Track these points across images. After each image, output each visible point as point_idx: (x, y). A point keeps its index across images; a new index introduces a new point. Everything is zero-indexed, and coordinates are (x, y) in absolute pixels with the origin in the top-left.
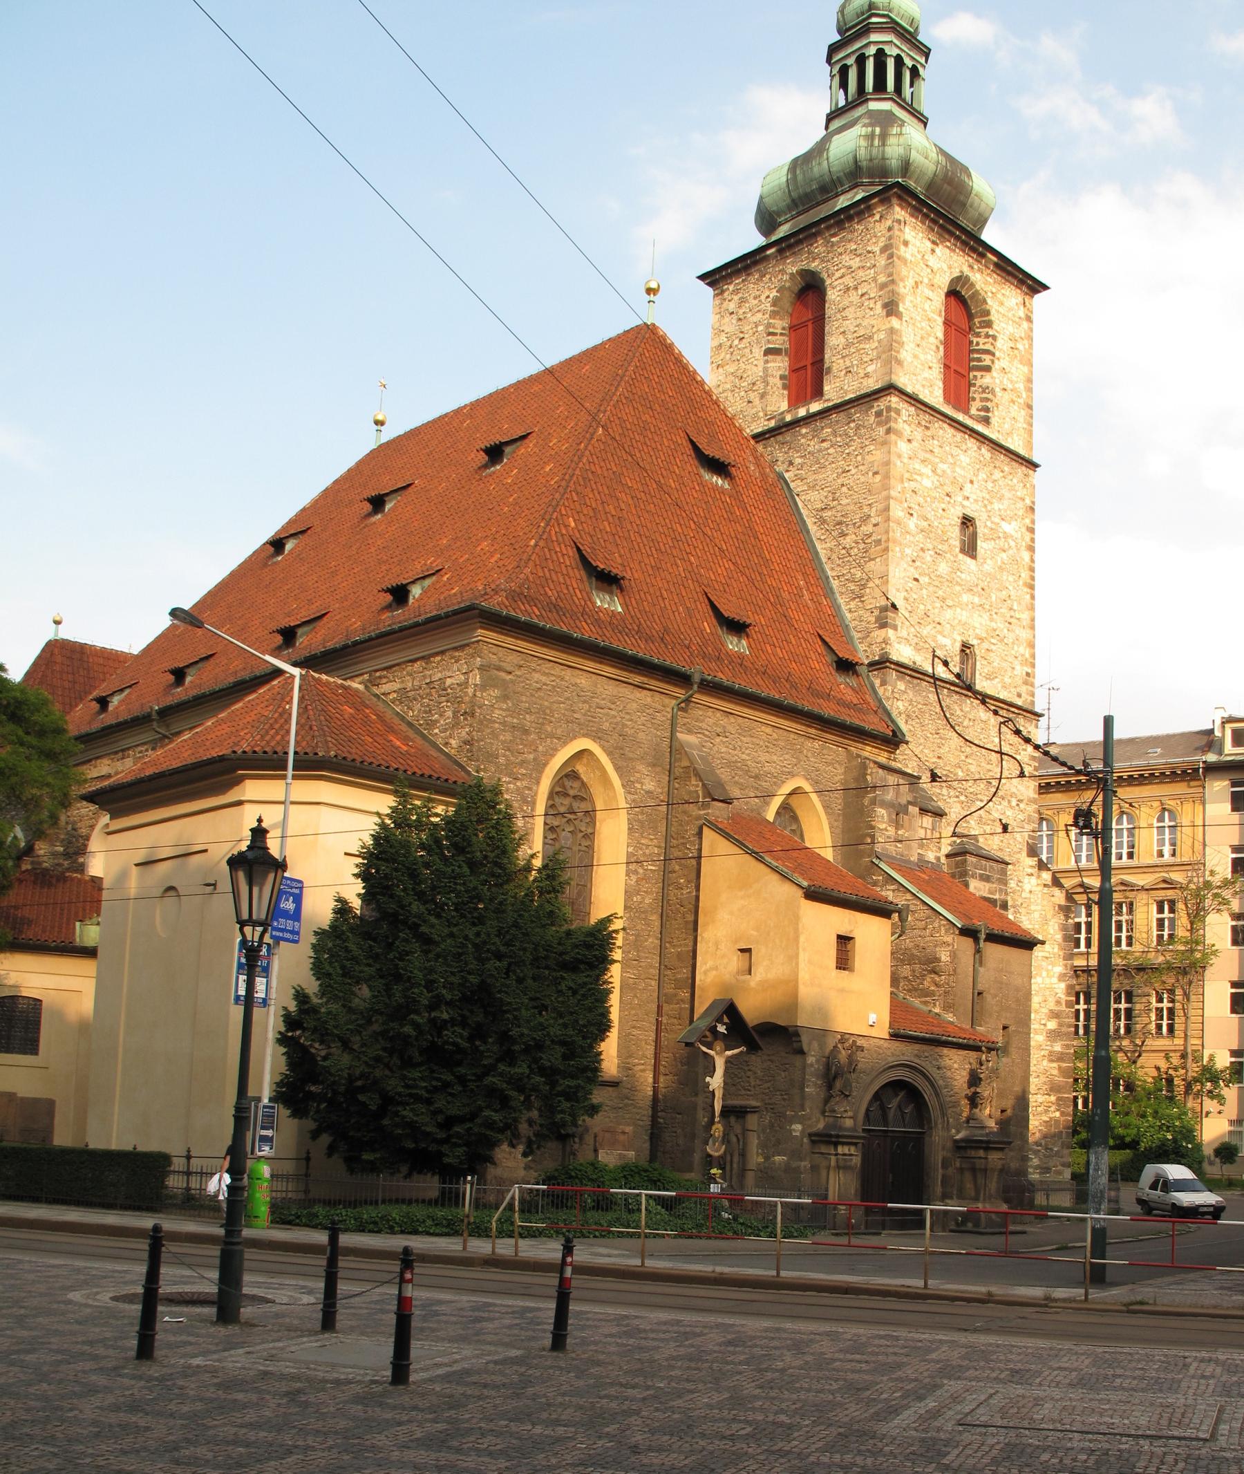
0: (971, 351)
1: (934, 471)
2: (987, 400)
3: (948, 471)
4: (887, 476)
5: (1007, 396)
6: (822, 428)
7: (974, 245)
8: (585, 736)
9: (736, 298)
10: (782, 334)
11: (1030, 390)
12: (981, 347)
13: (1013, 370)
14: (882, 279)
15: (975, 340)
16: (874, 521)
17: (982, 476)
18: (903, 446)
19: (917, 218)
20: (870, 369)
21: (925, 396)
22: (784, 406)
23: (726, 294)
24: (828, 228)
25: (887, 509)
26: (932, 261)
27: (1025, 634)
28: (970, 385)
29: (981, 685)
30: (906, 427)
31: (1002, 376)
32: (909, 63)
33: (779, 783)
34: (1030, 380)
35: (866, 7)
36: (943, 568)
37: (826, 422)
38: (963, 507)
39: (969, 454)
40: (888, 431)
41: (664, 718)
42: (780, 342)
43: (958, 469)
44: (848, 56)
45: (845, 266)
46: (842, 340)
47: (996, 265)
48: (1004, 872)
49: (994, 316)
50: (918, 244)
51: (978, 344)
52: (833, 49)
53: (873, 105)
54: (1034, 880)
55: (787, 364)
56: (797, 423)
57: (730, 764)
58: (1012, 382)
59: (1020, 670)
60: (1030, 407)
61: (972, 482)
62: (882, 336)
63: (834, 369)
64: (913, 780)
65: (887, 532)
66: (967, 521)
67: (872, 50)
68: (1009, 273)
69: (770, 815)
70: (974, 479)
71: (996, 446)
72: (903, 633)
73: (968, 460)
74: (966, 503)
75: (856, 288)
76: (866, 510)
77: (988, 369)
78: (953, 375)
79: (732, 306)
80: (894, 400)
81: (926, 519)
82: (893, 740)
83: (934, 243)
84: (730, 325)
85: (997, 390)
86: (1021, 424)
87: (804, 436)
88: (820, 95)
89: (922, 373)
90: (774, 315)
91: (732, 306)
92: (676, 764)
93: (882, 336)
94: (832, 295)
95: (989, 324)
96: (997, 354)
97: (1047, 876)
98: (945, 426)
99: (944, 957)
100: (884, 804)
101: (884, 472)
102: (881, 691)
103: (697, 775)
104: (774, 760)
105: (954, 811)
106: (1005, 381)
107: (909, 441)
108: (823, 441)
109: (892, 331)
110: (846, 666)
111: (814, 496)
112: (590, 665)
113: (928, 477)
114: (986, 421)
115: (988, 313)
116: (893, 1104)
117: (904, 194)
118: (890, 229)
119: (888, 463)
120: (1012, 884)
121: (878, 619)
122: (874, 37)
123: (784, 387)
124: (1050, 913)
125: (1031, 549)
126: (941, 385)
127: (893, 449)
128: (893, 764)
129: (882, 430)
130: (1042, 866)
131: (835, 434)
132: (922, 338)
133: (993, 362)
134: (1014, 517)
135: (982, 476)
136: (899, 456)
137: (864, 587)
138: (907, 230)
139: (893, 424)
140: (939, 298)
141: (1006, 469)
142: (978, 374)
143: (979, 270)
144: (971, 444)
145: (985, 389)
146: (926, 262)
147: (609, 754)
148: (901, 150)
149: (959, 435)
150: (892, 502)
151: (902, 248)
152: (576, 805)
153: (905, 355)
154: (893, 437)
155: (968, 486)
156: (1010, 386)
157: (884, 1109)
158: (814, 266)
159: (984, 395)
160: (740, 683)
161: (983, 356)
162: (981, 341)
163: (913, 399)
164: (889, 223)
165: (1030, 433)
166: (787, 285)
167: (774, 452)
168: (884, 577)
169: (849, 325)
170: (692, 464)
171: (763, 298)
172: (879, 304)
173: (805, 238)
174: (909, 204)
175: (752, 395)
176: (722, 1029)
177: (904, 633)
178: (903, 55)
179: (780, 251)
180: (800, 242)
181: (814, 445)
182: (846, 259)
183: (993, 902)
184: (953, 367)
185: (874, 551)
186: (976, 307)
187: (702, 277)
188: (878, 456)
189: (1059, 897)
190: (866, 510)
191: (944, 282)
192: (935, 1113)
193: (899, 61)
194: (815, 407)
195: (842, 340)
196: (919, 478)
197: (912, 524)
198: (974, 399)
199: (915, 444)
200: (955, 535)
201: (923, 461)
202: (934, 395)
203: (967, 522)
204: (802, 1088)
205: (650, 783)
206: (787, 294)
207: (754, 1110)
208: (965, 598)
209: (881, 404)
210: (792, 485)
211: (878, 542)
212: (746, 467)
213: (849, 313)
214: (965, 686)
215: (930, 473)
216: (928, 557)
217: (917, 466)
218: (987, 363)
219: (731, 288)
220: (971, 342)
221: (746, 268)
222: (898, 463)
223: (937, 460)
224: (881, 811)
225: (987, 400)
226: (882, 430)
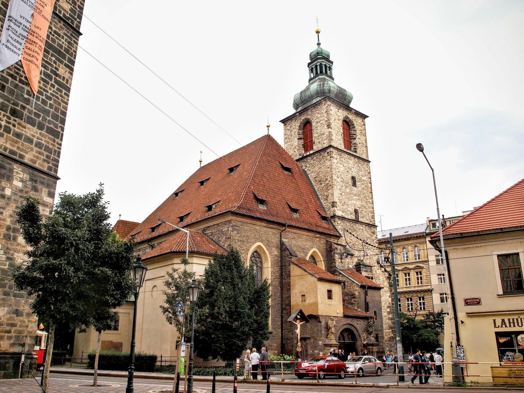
4: (331, 168)
5: (361, 145)
7: (348, 108)
8: (259, 241)
11: (366, 143)
14: (326, 119)
17: (356, 166)
18: (335, 161)
20: (325, 142)
21: (339, 147)
22: (303, 152)
25: (332, 177)
26: (338, 114)
27: (371, 205)
29: (361, 219)
31: (359, 140)
32: (328, 66)
33: (309, 250)
34: (366, 140)
36: (348, 190)
39: (352, 161)
40: (331, 157)
41: (278, 235)
42: (301, 136)
46: (317, 135)
48: (371, 269)
53: (320, 77)
54: (379, 270)
56: (307, 156)
57: (297, 246)
59: (371, 215)
60: (367, 147)
62: (327, 133)
63: (316, 142)
64: (344, 246)
66: (353, 178)
67: (318, 64)
69: (308, 259)
71: (359, 158)
72: (339, 208)
77: (355, 139)
80: (331, 149)
82: (338, 237)
84: (288, 133)
86: (365, 151)
88: (306, 74)
89: (338, 141)
91: (288, 128)
92: (282, 248)
93: (327, 133)
94: (314, 124)
95: (354, 127)
97: (383, 269)
99: (357, 294)
100: (337, 254)
102: (334, 224)
103: (288, 249)
104: (308, 244)
105: (356, 253)
109: (330, 132)
110: (324, 218)
111: (313, 174)
112: (259, 223)
114: (356, 152)
116: (345, 335)
117: (330, 98)
119: (331, 165)
120: (374, 272)
121: (332, 205)
122: (319, 61)
124: (385, 279)
125: (371, 183)
128: (339, 243)
129: (329, 157)
130: (381, 266)
131: (317, 158)
134: (365, 175)
135: (356, 166)
137: (327, 197)
140: (341, 123)
144: (352, 158)
145: (355, 144)
146: (337, 115)
147: (265, 246)
148: (328, 87)
149: (349, 156)
152: (257, 259)
153: (333, 138)
157: (343, 336)
158: (309, 117)
160: (298, 225)
163: (336, 149)
165: (367, 153)
168: (332, 194)
169: (318, 131)
170: (281, 170)
175: (295, 150)
176: (299, 317)
177: (339, 208)
181: (312, 162)
183: (369, 278)
185: (329, 188)
188: (328, 163)
189: (387, 275)
191: (342, 118)
192: (357, 337)
193: (326, 66)
194: (311, 152)
195: (317, 135)
197: (339, 180)
200: (350, 182)
202: (342, 147)
203: (353, 178)
204: (321, 332)
205: (276, 252)
207: (309, 338)
208: (354, 197)
209: (328, 151)
211: (330, 185)
212: (295, 170)
213: (318, 128)
214: (356, 221)
216: (344, 188)
224: (336, 256)
226: (329, 157)
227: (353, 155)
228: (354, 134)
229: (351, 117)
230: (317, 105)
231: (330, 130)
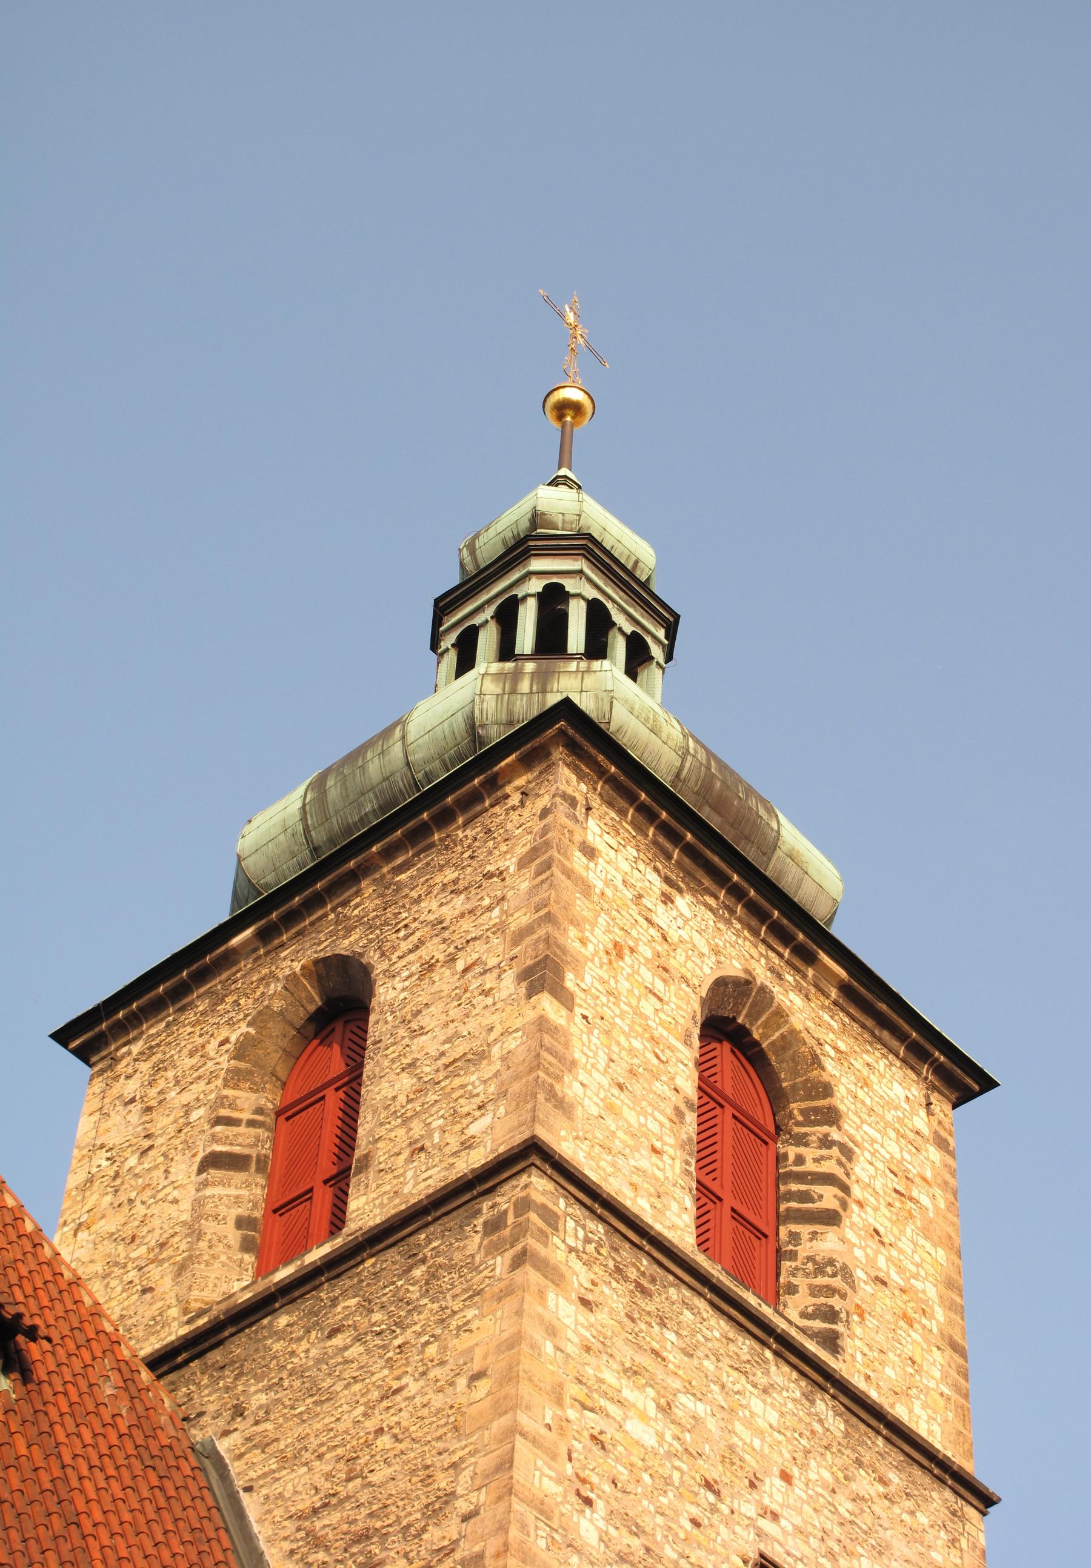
0: (781, 1179)
1: (666, 1409)
2: (831, 1291)
3: (711, 1424)
4: (510, 1376)
5: (885, 1302)
6: (334, 1302)
9: (145, 1067)
10: (251, 1123)
12: (810, 1166)
13: (904, 1244)
15: (792, 1152)
16: (462, 1506)
18: (563, 1309)
19: (622, 813)
23: (120, 1067)
24: (388, 854)
25: (507, 1463)
26: (662, 915)
28: (780, 1255)
30: (577, 1265)
35: (525, 524)
37: (345, 1282)
38: (760, 1534)
39: (772, 1406)
43: (739, 1427)
44: (479, 609)
45: (433, 954)
46: (406, 1082)
47: (845, 989)
49: (841, 1099)
50: (625, 866)
51: (800, 1160)
52: (444, 606)
55: (259, 1193)
58: (901, 1270)
61: (786, 1477)
63: (381, 1156)
65: (502, 1528)
67: (536, 586)
68: (883, 1022)
70: (796, 1472)
73: (773, 1417)
74: (765, 1524)
75: (452, 959)
76: (442, 1481)
77: (831, 1218)
78: (728, 1224)
79: (130, 1088)
80: (538, 1185)
81: (638, 1531)
83: (667, 880)
85: (859, 1274)
87: (279, 1335)
90: (235, 1078)
91: (130, 1088)
95: (832, 1117)
96: (856, 1191)
98: (701, 1304)
101: (506, 1371)
106: (881, 1262)
107: (585, 1302)
108: (334, 1332)
109: (542, 1024)
113: (644, 1416)
114: (831, 1341)
115: (827, 1090)
118: (545, 813)
119: (514, 1341)
123: (247, 1246)
126: (689, 1202)
127: (531, 1303)
129: (501, 1263)
132: (632, 1073)
133: (844, 1205)
135: (820, 1471)
136: (552, 1332)
138: (592, 823)
139: (531, 1242)
141: (893, 1476)
142: (805, 1230)
143: (799, 988)
144: (781, 1374)
149: (745, 1346)
150: (519, 1442)
151: (578, 861)
154: (530, 1275)
155: (773, 1490)
156: (895, 1277)
158: (344, 946)
159: (821, 1280)
161: (818, 1189)
162: (809, 1153)
164: (544, 801)
166: (277, 1005)
167: (203, 1390)
171: (212, 1048)
172: (509, 977)
173: (332, 890)
174: (601, 772)
178: (609, 605)
179: (265, 936)
180: (316, 901)
181: (308, 1349)
182: (431, 908)
184: (729, 1201)
186: (795, 1073)
187: (62, 1037)
190: (442, 1481)
195: (406, 1082)
196: (613, 1409)
197: (589, 1528)
198: (792, 1290)
199: (601, 1316)
201: (632, 1372)
206: (275, 1028)
209: (505, 1199)
210: (234, 1468)
215: (652, 1410)
217: (610, 1377)
218: (828, 1197)
219: (136, 1048)
220: (780, 1158)
221: (179, 993)
222: (549, 1348)
223: (677, 1384)
225: (831, 1291)
226: (501, 1263)
227: (787, 1348)
228: (828, 1179)
229: (805, 1011)
230: (445, 818)
231: (546, 1003)
